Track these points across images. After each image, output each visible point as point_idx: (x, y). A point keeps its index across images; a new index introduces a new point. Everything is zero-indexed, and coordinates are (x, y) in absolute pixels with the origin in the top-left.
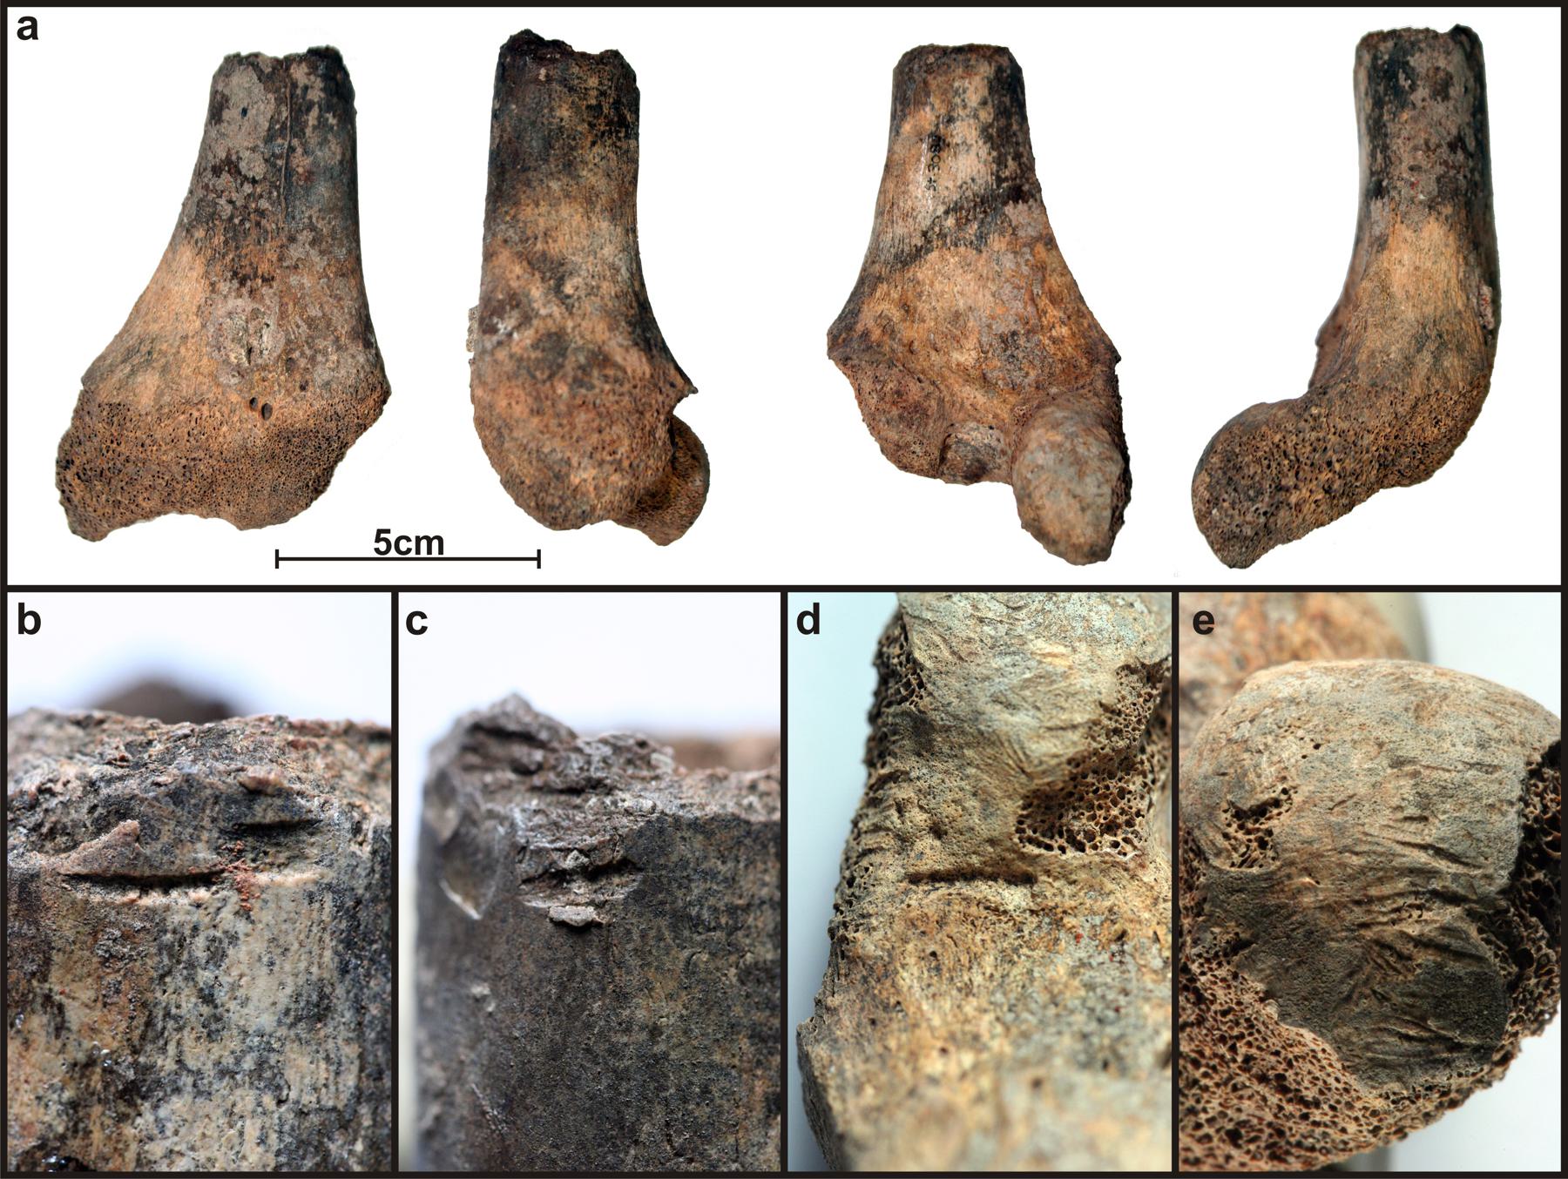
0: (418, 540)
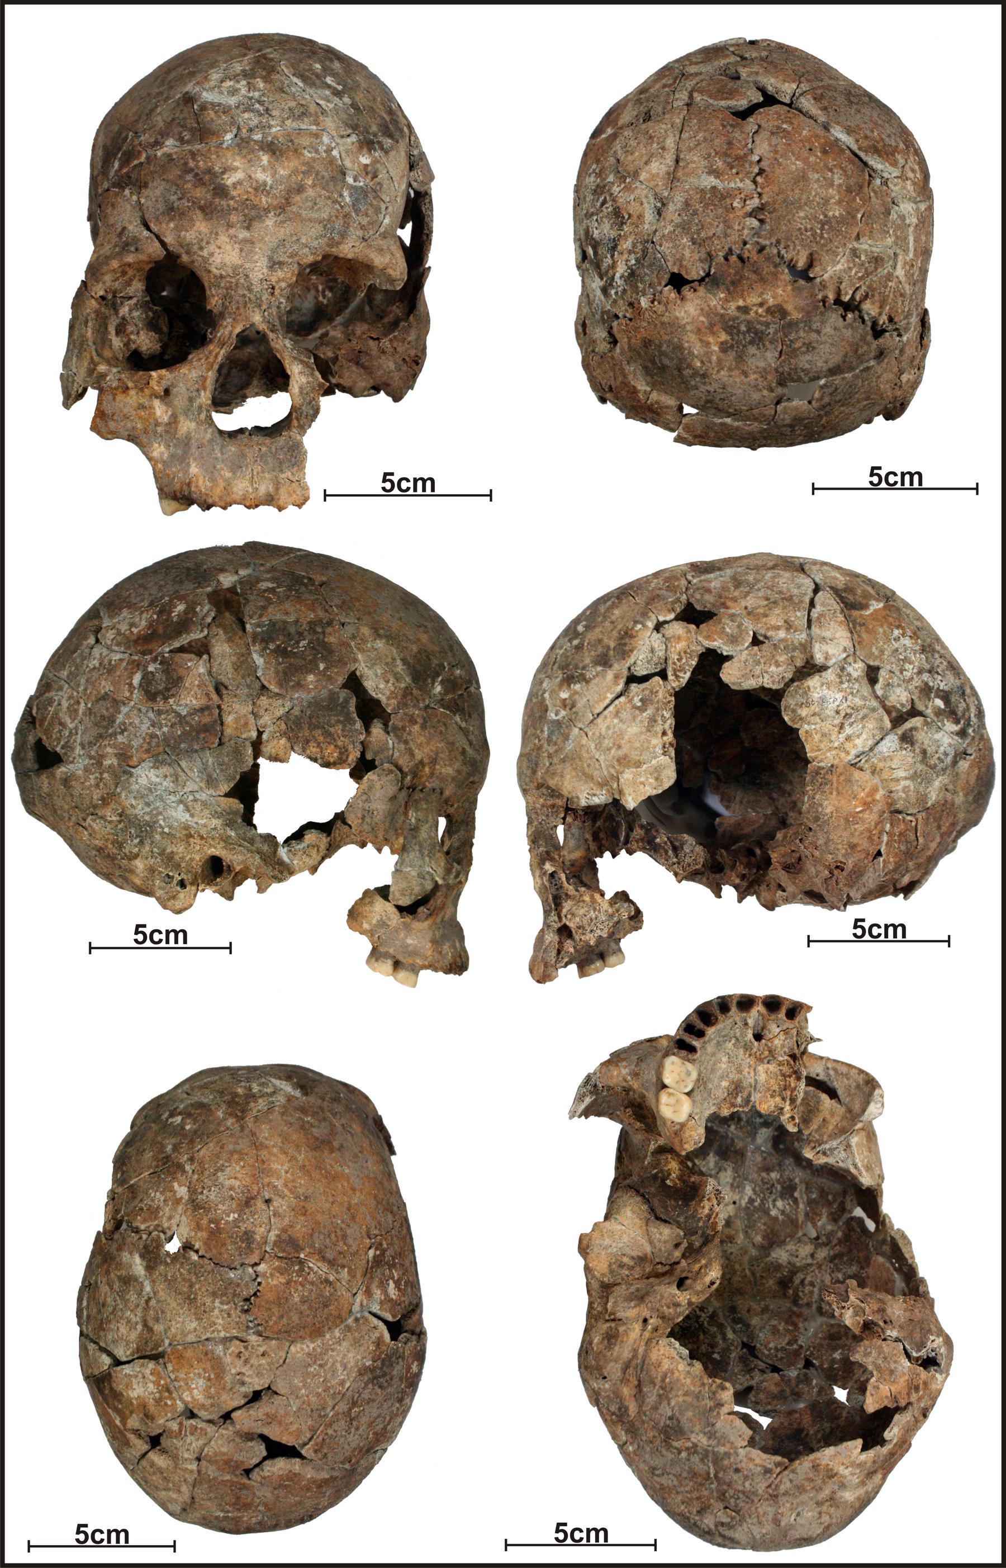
0: (168, 932)
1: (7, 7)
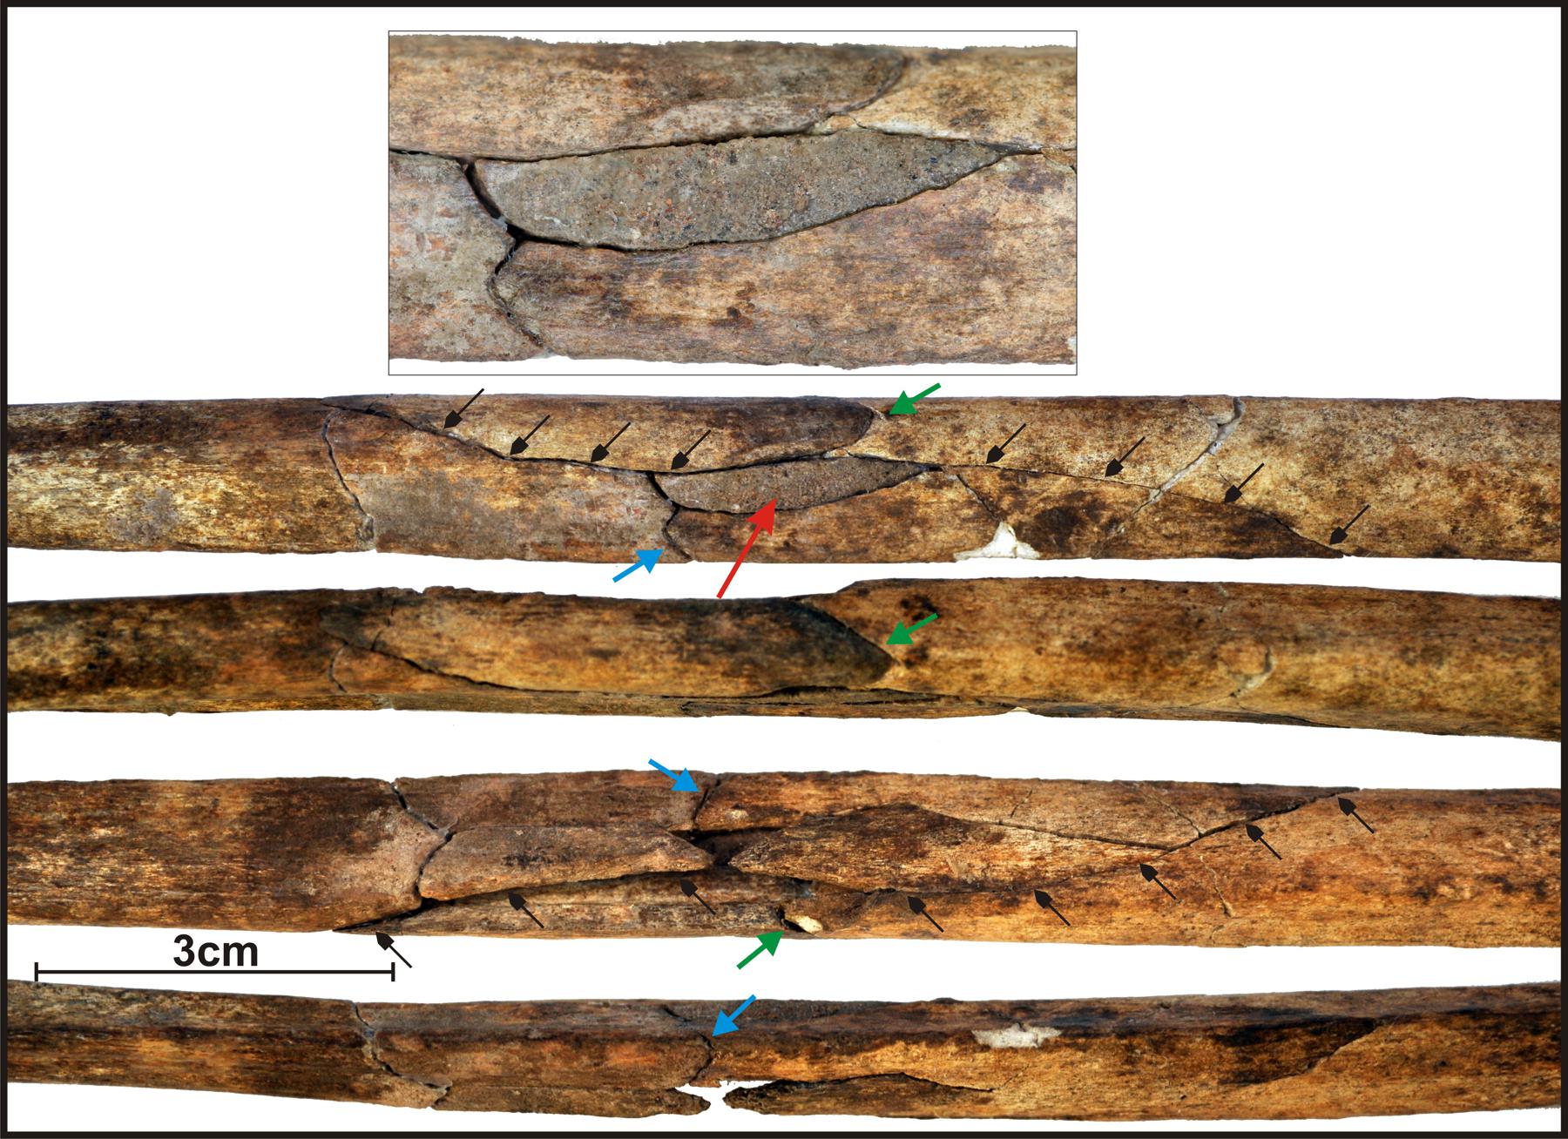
0: (227, 947)
1: (10, 10)
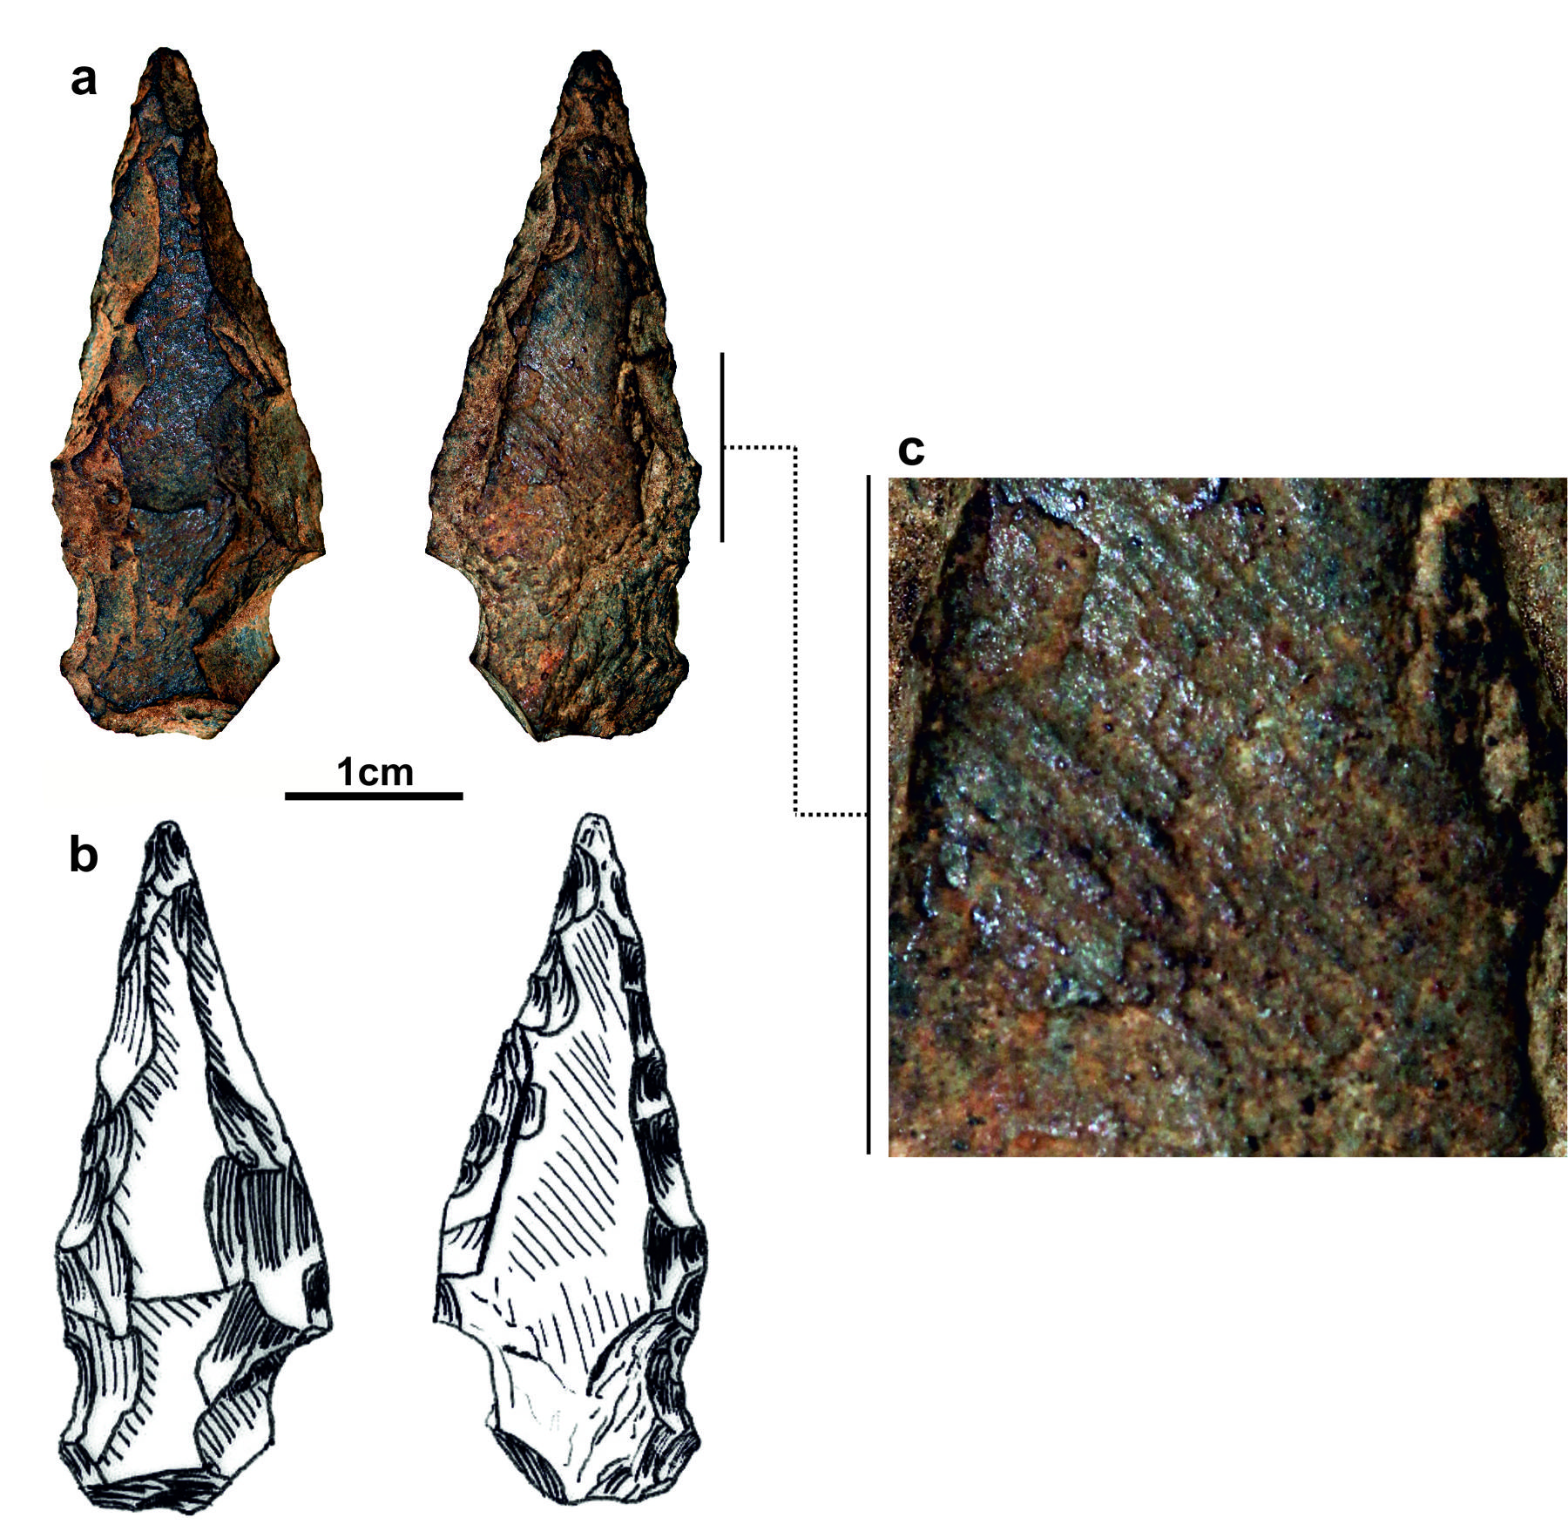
0: (385, 769)
